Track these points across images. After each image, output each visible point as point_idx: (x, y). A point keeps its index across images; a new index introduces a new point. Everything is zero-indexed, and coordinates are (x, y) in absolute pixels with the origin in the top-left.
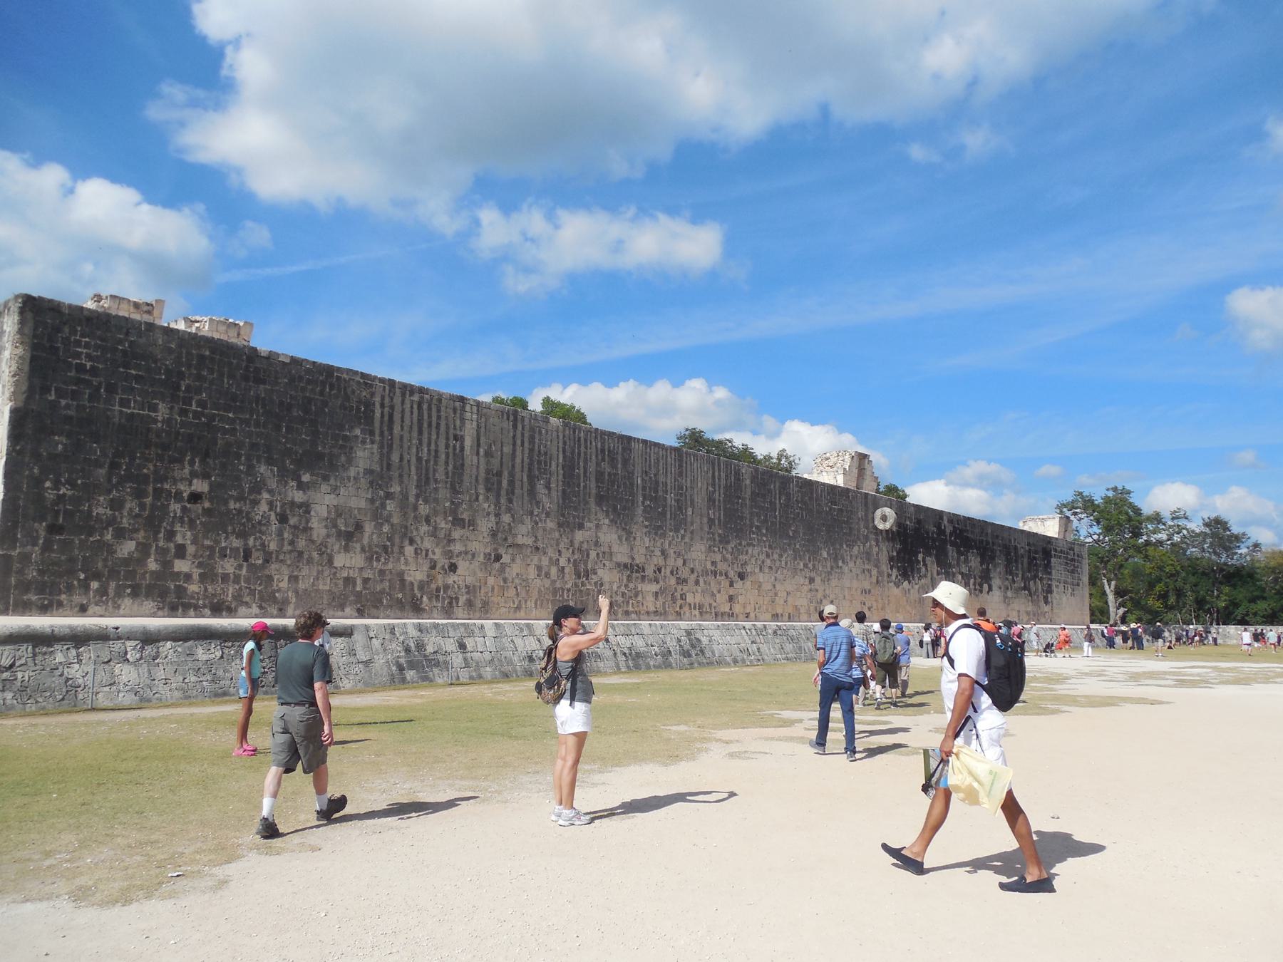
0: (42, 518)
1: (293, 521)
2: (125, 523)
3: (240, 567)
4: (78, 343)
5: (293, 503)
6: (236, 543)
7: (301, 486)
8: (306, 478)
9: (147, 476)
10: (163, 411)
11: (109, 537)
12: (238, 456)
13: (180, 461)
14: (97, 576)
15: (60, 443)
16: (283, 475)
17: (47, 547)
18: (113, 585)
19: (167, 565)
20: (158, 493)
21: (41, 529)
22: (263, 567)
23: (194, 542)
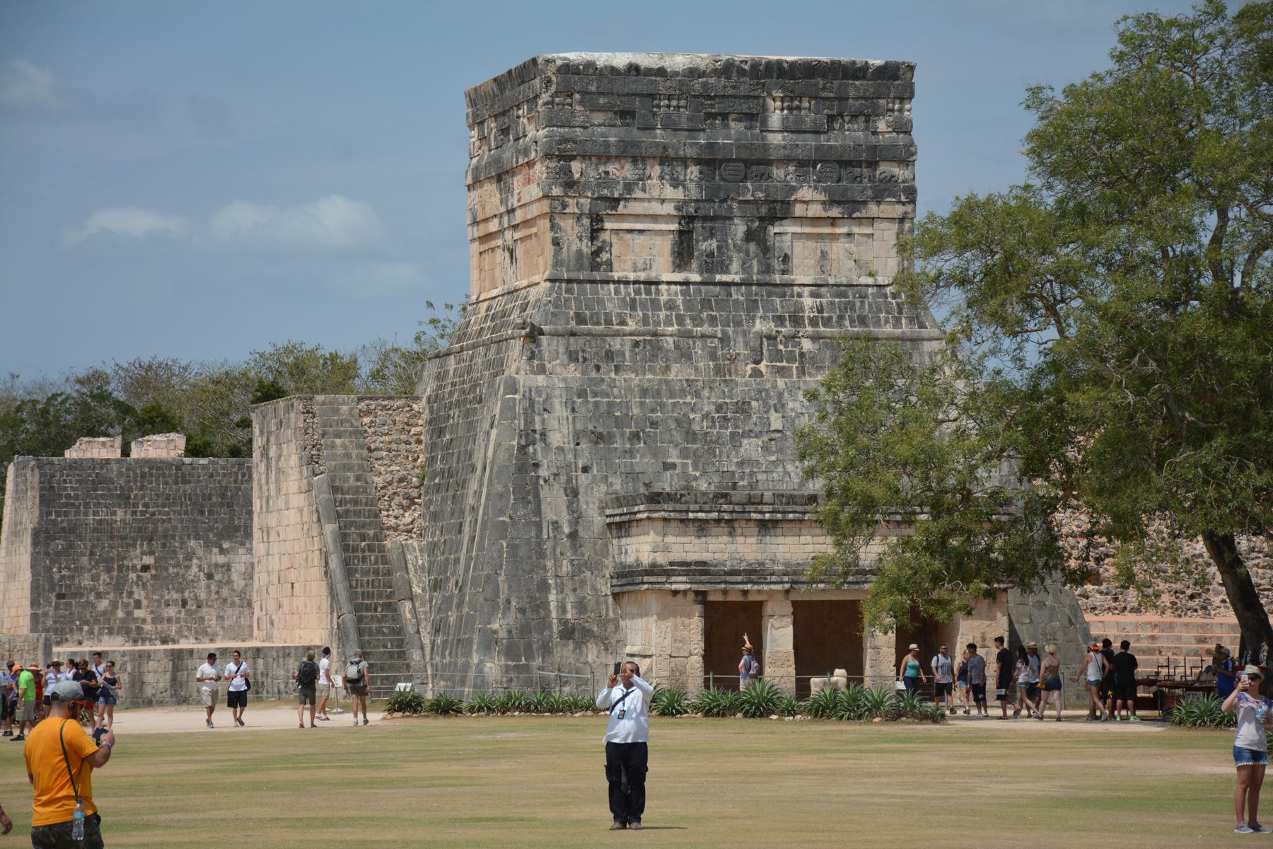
0: (52, 590)
1: (217, 577)
2: (101, 589)
3: (179, 612)
4: (65, 481)
5: (216, 565)
6: (176, 596)
7: (222, 551)
8: (226, 545)
9: (113, 559)
10: (120, 513)
11: (92, 598)
12: (173, 537)
13: (134, 546)
14: (87, 623)
15: (60, 544)
16: (208, 546)
17: (57, 607)
18: (96, 628)
19: (129, 614)
20: (120, 568)
21: (53, 597)
22: (196, 611)
23: (146, 598)
